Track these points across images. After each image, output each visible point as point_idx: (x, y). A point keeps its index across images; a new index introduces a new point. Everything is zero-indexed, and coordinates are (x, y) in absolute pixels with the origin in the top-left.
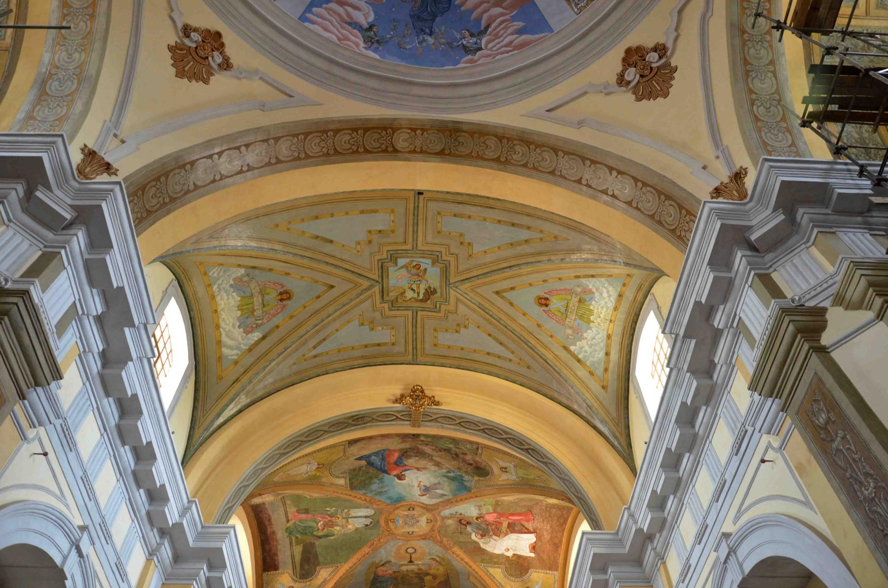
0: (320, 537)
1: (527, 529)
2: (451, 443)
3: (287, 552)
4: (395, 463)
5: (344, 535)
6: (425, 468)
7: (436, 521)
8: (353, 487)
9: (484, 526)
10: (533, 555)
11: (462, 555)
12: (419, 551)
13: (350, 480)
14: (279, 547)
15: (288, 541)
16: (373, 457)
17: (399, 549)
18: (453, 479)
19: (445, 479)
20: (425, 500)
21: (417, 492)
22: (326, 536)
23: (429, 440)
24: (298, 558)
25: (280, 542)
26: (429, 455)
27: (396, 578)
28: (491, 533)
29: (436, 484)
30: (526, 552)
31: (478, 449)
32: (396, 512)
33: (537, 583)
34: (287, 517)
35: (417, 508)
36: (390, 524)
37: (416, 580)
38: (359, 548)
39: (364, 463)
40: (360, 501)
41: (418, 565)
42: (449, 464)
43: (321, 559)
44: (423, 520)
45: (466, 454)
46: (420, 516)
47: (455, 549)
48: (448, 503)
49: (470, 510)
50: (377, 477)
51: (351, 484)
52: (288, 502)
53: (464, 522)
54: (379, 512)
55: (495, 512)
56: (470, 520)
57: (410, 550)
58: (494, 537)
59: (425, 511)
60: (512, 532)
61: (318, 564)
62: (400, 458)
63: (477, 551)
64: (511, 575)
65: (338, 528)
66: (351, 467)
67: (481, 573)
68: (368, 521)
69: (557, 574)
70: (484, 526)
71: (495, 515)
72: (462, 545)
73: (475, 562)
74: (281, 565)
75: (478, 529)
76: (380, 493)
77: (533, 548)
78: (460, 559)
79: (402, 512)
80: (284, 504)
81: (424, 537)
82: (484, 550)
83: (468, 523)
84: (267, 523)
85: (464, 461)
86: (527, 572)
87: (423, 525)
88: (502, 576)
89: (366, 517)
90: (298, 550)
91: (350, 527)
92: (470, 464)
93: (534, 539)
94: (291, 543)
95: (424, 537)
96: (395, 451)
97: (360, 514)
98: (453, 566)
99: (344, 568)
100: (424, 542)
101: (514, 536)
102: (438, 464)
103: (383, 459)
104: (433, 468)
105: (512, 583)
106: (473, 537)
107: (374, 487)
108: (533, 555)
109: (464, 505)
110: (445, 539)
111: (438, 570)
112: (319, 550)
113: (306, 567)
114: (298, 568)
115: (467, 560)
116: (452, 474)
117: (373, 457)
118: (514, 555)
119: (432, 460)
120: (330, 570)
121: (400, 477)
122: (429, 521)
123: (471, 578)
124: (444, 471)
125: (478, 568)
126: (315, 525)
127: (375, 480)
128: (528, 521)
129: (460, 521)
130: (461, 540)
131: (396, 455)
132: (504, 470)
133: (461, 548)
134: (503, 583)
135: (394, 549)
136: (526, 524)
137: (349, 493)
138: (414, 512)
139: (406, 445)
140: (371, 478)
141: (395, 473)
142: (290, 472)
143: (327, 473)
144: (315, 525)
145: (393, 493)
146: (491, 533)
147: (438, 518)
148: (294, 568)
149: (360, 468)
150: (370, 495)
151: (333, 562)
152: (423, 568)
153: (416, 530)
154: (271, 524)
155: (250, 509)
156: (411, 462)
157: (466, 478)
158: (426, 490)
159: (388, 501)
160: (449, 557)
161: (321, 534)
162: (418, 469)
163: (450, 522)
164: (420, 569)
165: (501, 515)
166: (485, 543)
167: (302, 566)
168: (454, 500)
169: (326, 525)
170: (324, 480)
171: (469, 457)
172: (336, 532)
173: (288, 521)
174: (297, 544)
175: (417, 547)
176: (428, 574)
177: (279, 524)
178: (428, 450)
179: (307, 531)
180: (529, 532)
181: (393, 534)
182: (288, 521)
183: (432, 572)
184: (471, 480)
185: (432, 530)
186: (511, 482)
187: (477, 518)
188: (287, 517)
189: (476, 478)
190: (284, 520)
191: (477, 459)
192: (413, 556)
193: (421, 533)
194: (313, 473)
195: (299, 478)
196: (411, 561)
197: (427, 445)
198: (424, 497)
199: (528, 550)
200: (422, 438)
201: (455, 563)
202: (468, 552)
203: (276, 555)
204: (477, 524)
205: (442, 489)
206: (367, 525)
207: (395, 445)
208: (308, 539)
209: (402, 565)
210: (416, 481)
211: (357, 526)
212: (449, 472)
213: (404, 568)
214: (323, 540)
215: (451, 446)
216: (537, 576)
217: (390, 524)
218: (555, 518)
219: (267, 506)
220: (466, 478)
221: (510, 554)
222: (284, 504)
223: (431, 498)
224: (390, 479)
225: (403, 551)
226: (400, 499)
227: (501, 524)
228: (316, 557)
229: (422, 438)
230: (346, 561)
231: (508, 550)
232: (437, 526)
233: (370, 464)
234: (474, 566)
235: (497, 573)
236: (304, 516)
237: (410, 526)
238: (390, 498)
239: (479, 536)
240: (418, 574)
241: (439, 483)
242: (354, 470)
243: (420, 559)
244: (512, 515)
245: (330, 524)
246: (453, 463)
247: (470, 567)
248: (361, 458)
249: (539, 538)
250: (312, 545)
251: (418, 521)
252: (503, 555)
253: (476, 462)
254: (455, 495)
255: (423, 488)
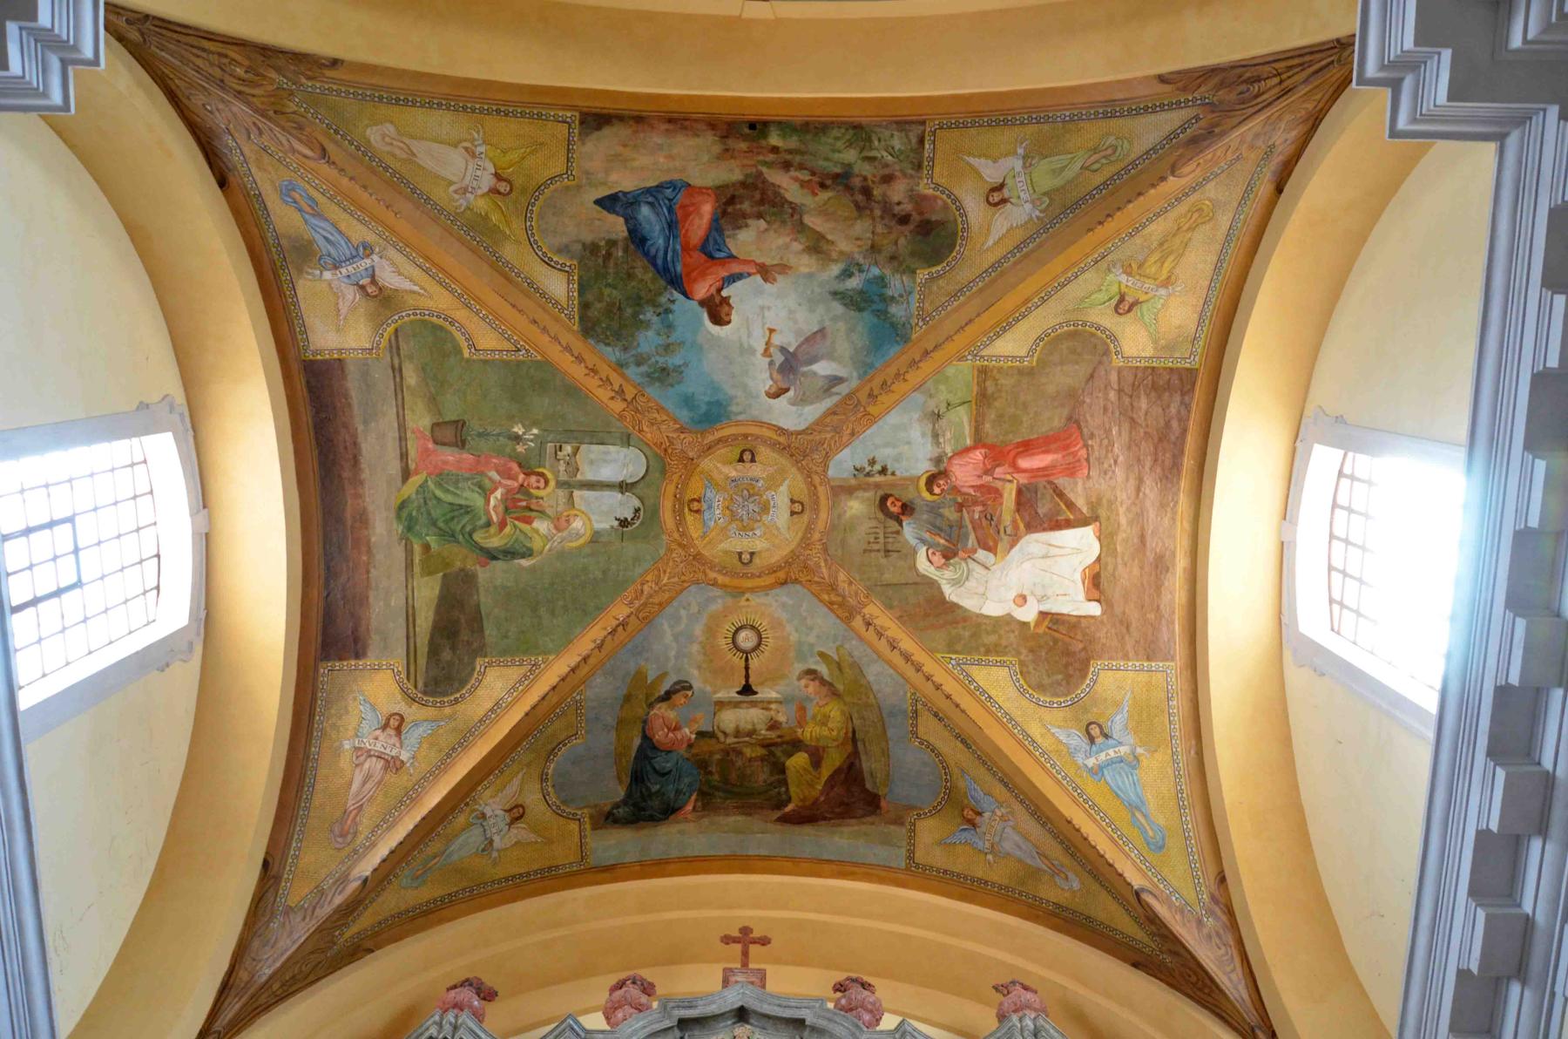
0: (491, 555)
1: (1070, 505)
2: (850, 145)
3: (397, 594)
4: (704, 248)
5: (562, 555)
6: (784, 268)
7: (816, 509)
8: (589, 328)
9: (950, 514)
10: (1095, 609)
11: (894, 630)
12: (770, 642)
13: (582, 289)
14: (374, 573)
15: (399, 553)
16: (645, 211)
17: (711, 631)
18: (855, 302)
19: (838, 308)
20: (789, 415)
21: (762, 380)
22: (510, 553)
23: (793, 142)
24: (425, 621)
25: (379, 556)
26: (795, 209)
27: (703, 765)
28: (972, 541)
29: (810, 339)
30: (1076, 603)
31: (921, 141)
32: (707, 464)
33: (1118, 705)
34: (404, 456)
35: (764, 452)
36: (689, 518)
37: (762, 776)
38: (600, 609)
39: (616, 226)
40: (603, 394)
41: (765, 705)
42: (849, 235)
43: (490, 631)
44: (780, 499)
45: (888, 179)
46: (773, 482)
47: (873, 610)
48: (854, 410)
49: (905, 442)
50: (655, 305)
51: (585, 306)
52: (411, 378)
53: (894, 507)
54: (661, 461)
55: (979, 443)
56: (910, 494)
57: (746, 639)
58: (981, 554)
59: (784, 461)
60: (1031, 528)
61: (481, 651)
62: (716, 227)
63: (935, 613)
64: (1040, 687)
65: (542, 526)
66: (588, 237)
67: (950, 686)
68: (624, 505)
69: (1171, 671)
70: (950, 514)
71: (978, 455)
72: (888, 592)
73: (931, 652)
74: (375, 641)
75: (936, 529)
76: (663, 375)
77: (1096, 582)
78: (893, 657)
79: (719, 466)
80: (397, 371)
81: (788, 574)
82: (954, 607)
83: (907, 509)
84: (346, 474)
85: (887, 208)
86: (1084, 672)
87: (775, 533)
88: (1012, 692)
89: (623, 487)
90: (427, 591)
91: (577, 524)
92: (904, 220)
93: (1094, 549)
94: (409, 565)
95: (788, 574)
96: (701, 190)
97: (607, 473)
98: (869, 687)
99: (556, 670)
100: (783, 595)
101: (1034, 542)
102: (818, 246)
103: (672, 226)
104: (806, 264)
105: (1047, 715)
106: (923, 565)
107: (648, 340)
108: (1095, 609)
109: (893, 418)
110: (842, 576)
111: (824, 721)
112: (485, 600)
113: (446, 655)
114: (422, 661)
115: (907, 644)
116: (854, 283)
117: (645, 211)
118: (1043, 614)
119: (801, 228)
120: (514, 673)
121: (718, 311)
122: (797, 508)
123: (928, 727)
124: (836, 269)
125: (940, 670)
126: (479, 501)
127: (649, 314)
128: (1071, 471)
129: (884, 499)
130: (888, 577)
131: (707, 209)
132: (996, 196)
133: (890, 607)
134: (1017, 714)
135: (698, 630)
136: (1062, 481)
137: (578, 345)
138: (756, 470)
139: (730, 173)
140: (638, 302)
141: (702, 289)
142: (418, 147)
143: (517, 225)
144: (479, 501)
145: (691, 386)
146: (972, 541)
147: (821, 489)
148: (411, 653)
149: (612, 243)
150: (632, 372)
151: (525, 647)
152: (782, 718)
153: (759, 545)
154: (357, 482)
155: (300, 382)
156: (746, 241)
157: (896, 284)
158: (789, 366)
159: (684, 415)
160: (856, 648)
161: (495, 542)
162: (765, 272)
163: (856, 507)
164: (774, 725)
165: (998, 455)
166: (956, 583)
167: (434, 651)
168: (863, 395)
169: (509, 505)
170: (509, 252)
171: (898, 192)
172: (537, 544)
173: (406, 474)
174: (428, 571)
175: (763, 624)
176: (796, 745)
177: (380, 490)
178: (788, 185)
179: (455, 524)
180: (1083, 522)
181: (698, 557)
182: (406, 474)
183: (809, 733)
184: (909, 291)
185: (806, 542)
186: (1019, 236)
187: (931, 480)
188: (404, 456)
189: (922, 274)
190: (395, 467)
191: (924, 188)
192: (754, 663)
193: (777, 557)
194: (482, 205)
195: (439, 194)
196: (747, 690)
197: (787, 166)
198: (783, 400)
199: (1079, 592)
200: (774, 139)
201: (876, 673)
202: (907, 618)
203: (363, 601)
204: (934, 509)
205: (830, 356)
206: (624, 523)
207: (702, 165)
208: (461, 558)
209: (721, 705)
210: (767, 318)
211: (598, 526)
212: (847, 274)
213: (730, 719)
214: (499, 565)
215: (850, 156)
216: (1117, 682)
217: (689, 518)
218: (1147, 447)
219: (353, 384)
220: (896, 284)
221: (1028, 614)
222: (397, 371)
223: (801, 401)
224: (687, 311)
225: (723, 643)
226: (713, 413)
227: (997, 494)
228: (476, 620)
229: (774, 139)
230: (567, 641)
231: (1022, 599)
232: (820, 525)
233: (637, 238)
234: (929, 666)
235: (998, 680)
236: (449, 456)
237: (746, 529)
238: (688, 401)
239: (938, 559)
240: (768, 745)
241: (822, 332)
242: (593, 249)
243: (773, 678)
244: (1027, 447)
245: (520, 507)
246: (862, 227)
247: (918, 669)
248: (609, 203)
249: (1105, 538)
250: (468, 579)
251: (765, 508)
252: (1008, 620)
253: (919, 200)
254: (865, 369)
255: (779, 358)
